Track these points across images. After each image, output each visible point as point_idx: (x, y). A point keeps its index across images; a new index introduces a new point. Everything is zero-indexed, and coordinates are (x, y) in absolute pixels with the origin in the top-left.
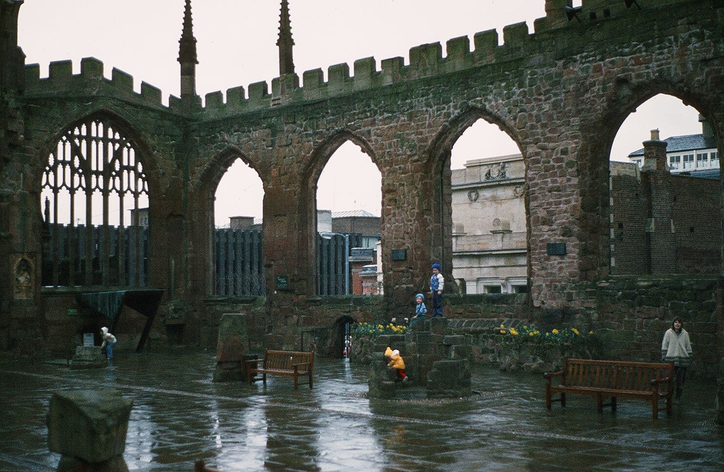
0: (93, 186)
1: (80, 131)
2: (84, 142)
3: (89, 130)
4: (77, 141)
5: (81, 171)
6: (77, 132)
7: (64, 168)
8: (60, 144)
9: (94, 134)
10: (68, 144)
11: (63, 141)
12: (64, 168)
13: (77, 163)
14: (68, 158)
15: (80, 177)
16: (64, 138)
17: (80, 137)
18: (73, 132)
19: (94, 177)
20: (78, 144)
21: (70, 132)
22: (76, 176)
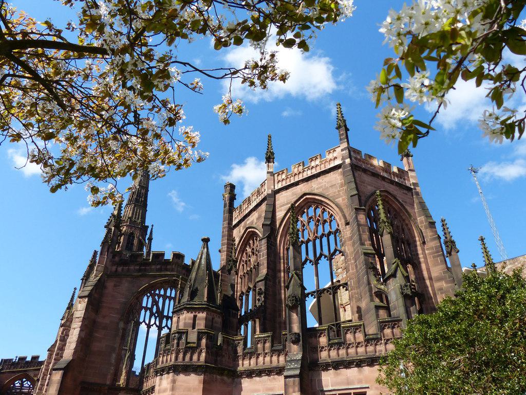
0: (164, 325)
1: (159, 292)
2: (161, 300)
3: (165, 292)
4: (156, 297)
5: (156, 315)
6: (157, 292)
7: (146, 312)
8: (145, 298)
9: (168, 294)
10: (150, 299)
11: (147, 296)
12: (146, 312)
13: (155, 310)
14: (149, 306)
15: (156, 318)
16: (149, 295)
17: (159, 296)
18: (154, 292)
19: (165, 319)
20: (157, 299)
21: (153, 292)
22: (153, 317)
